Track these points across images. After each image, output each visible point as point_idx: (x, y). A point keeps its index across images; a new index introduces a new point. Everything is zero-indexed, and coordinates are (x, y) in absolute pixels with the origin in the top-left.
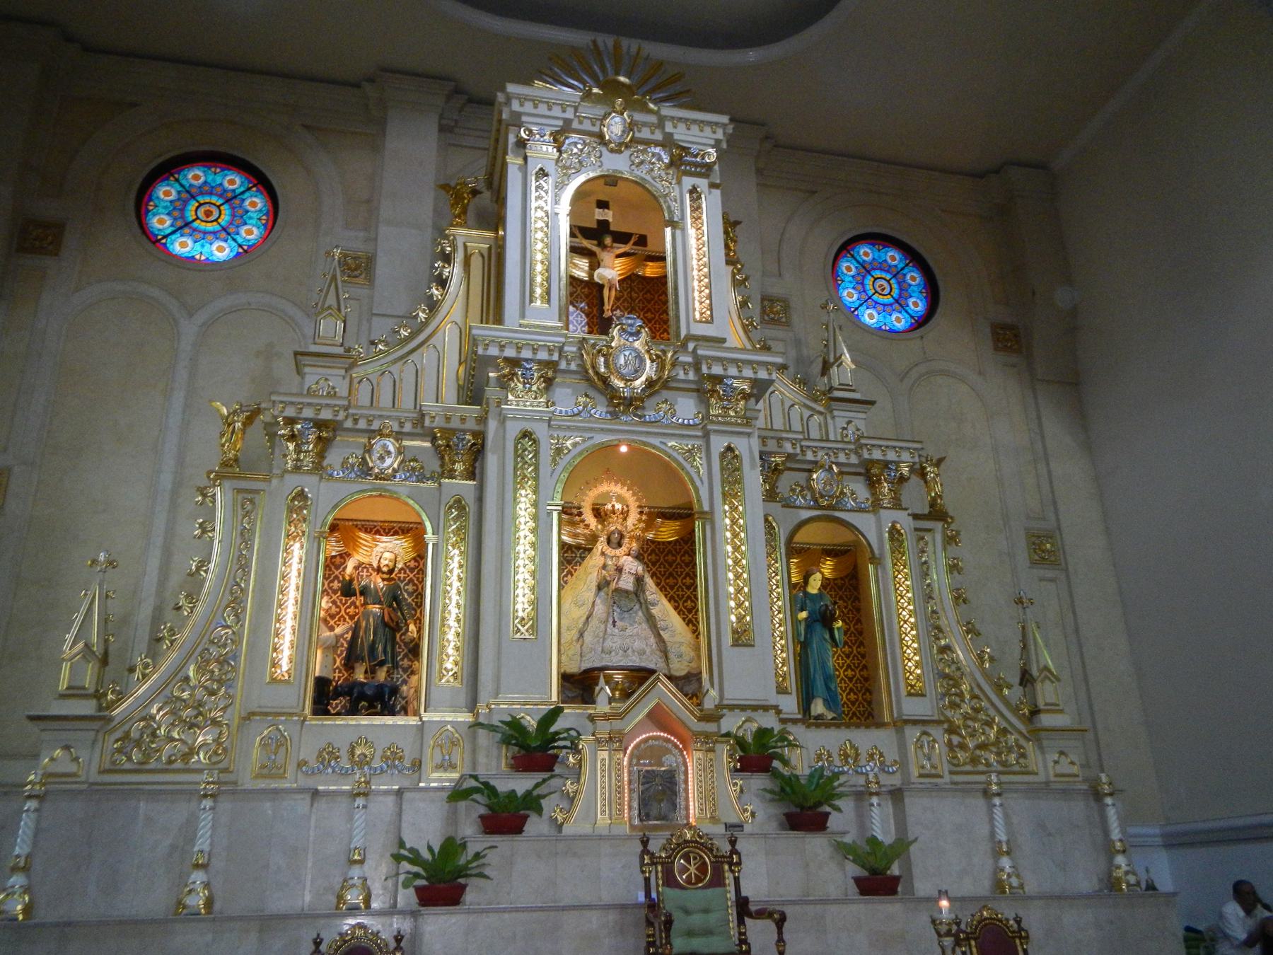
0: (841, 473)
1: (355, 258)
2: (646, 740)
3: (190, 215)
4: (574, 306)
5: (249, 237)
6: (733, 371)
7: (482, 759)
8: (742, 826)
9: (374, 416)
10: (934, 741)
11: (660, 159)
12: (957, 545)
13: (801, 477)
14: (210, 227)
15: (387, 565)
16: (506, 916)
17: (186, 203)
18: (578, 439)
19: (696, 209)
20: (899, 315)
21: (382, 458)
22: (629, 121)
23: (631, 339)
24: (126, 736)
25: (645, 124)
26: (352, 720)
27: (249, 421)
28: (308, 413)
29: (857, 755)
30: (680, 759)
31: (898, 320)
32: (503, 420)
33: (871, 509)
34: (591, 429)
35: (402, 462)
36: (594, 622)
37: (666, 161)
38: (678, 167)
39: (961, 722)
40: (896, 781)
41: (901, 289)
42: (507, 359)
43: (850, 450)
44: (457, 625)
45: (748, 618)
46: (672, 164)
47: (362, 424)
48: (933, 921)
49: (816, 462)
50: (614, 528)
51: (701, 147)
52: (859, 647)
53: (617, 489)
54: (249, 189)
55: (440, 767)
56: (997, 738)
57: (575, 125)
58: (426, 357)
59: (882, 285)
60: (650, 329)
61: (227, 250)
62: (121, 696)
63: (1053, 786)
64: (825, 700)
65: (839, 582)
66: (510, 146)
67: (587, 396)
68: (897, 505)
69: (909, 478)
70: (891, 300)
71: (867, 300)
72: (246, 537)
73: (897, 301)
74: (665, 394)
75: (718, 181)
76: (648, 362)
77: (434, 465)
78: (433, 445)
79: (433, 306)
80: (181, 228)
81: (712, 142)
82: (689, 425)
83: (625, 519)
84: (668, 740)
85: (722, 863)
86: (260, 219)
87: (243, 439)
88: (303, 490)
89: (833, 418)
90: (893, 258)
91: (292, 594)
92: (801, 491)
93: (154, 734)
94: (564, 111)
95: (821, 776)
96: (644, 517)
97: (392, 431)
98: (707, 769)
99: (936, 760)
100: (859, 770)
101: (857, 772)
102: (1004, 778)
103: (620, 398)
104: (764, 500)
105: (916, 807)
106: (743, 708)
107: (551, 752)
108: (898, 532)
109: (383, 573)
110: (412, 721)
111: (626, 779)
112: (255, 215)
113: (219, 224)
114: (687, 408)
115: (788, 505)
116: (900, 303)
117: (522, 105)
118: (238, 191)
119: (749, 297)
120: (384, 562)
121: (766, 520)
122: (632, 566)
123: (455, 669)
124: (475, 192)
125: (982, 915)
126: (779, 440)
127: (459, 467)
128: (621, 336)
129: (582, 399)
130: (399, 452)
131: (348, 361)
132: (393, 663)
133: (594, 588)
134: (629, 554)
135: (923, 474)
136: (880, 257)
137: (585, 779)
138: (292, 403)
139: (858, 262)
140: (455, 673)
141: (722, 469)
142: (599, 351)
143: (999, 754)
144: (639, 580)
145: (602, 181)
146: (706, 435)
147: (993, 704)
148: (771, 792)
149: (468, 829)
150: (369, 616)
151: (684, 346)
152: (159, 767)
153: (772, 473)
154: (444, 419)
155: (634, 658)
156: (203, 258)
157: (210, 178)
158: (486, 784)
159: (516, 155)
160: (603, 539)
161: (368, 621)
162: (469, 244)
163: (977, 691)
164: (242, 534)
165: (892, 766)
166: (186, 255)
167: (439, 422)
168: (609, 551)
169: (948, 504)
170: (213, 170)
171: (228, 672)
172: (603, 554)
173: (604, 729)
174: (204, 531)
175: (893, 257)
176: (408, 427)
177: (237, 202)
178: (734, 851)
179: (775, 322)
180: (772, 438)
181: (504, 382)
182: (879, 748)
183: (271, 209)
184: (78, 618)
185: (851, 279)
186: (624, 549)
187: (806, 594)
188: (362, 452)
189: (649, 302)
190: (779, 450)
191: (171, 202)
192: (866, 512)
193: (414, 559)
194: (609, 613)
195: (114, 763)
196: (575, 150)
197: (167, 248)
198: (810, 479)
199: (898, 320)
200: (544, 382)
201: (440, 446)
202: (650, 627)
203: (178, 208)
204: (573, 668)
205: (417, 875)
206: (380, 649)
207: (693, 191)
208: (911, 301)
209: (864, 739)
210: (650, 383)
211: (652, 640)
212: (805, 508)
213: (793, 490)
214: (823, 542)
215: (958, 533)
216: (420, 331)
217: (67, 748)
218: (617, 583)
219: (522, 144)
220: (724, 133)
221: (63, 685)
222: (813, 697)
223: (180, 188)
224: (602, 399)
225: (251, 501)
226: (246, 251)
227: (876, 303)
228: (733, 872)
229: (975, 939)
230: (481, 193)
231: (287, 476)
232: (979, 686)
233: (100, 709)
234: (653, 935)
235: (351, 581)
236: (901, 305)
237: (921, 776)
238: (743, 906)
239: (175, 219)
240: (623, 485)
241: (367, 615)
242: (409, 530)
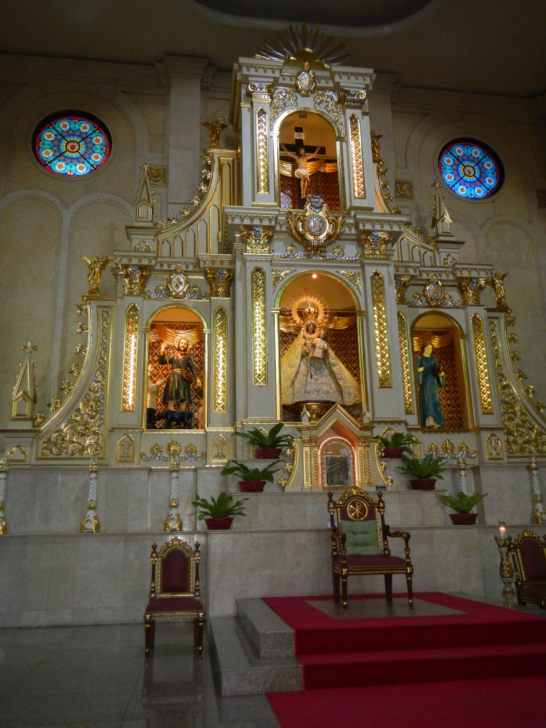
0: (443, 286)
1: (157, 170)
2: (330, 441)
3: (63, 149)
4: (284, 193)
6: (378, 227)
7: (239, 452)
8: (386, 488)
9: (171, 262)
10: (498, 439)
11: (332, 99)
12: (514, 326)
13: (420, 289)
14: (75, 155)
15: (183, 347)
16: (255, 535)
17: (60, 141)
18: (288, 271)
19: (354, 129)
20: (479, 188)
21: (177, 286)
22: (312, 76)
23: (317, 211)
24: (49, 441)
25: (322, 78)
26: (168, 432)
27: (103, 267)
28: (135, 261)
29: (453, 447)
30: (350, 451)
31: (479, 191)
32: (244, 262)
33: (462, 306)
34: (295, 265)
35: (189, 288)
36: (300, 376)
37: (336, 100)
38: (343, 104)
39: (515, 428)
40: (476, 462)
42: (245, 226)
43: (449, 272)
44: (223, 379)
45: (388, 372)
46: (339, 101)
47: (165, 267)
48: (496, 539)
49: (428, 280)
50: (310, 322)
51: (357, 90)
52: (454, 387)
53: (311, 300)
54: (95, 131)
55: (217, 456)
56: (536, 437)
57: (281, 81)
58: (200, 226)
59: (469, 170)
60: (329, 204)
61: (85, 169)
62: (44, 420)
64: (434, 417)
65: (443, 350)
66: (242, 97)
67: (292, 245)
68: (477, 303)
69: (485, 287)
70: (475, 179)
71: (460, 180)
72: (105, 332)
74: (338, 243)
75: (368, 111)
76: (327, 224)
77: (206, 289)
78: (205, 276)
79: (202, 196)
80: (58, 157)
81: (363, 86)
82: (352, 260)
83: (316, 317)
84: (343, 441)
85: (374, 507)
86: (102, 149)
88: (134, 306)
89: (439, 253)
91: (132, 363)
92: (420, 297)
93: (63, 440)
94: (273, 73)
95: (431, 459)
96: (327, 316)
97: (182, 270)
98: (365, 457)
99: (499, 450)
100: (454, 456)
101: (453, 457)
102: (539, 460)
103: (311, 246)
104: (397, 304)
105: (486, 476)
106: (386, 423)
107: (277, 448)
108: (478, 319)
109: (181, 351)
110: (201, 432)
111: (320, 462)
112: (98, 147)
113: (79, 153)
115: (412, 305)
116: (480, 181)
117: (248, 70)
118: (88, 133)
119: (387, 182)
120: (181, 345)
121: (399, 315)
122: (321, 343)
123: (223, 403)
124: (223, 126)
125: (524, 535)
126: (406, 267)
127: (220, 290)
128: (311, 209)
129: (289, 248)
130: (187, 282)
131: (156, 230)
132: (189, 400)
133: (299, 357)
134: (319, 337)
135: (493, 284)
136: (467, 152)
137: (297, 463)
138: (125, 256)
140: (223, 405)
141: (372, 285)
142: (299, 219)
143: (536, 446)
144: (325, 352)
145: (298, 115)
146: (363, 266)
147: (534, 418)
148: (402, 468)
149: (233, 489)
150: (175, 375)
151: (349, 213)
152: (68, 456)
153: (402, 287)
154: (211, 263)
155: (323, 396)
156: (72, 174)
158: (242, 465)
159: (246, 102)
160: (304, 329)
161: (174, 378)
162: (221, 158)
163: (525, 411)
164: (103, 330)
165: (473, 454)
166: (62, 172)
167: (208, 264)
168: (308, 336)
169: (509, 302)
170: (74, 121)
171: (100, 406)
172: (304, 337)
173: (306, 435)
174: (83, 330)
175: (476, 152)
176: (191, 268)
178: (381, 501)
179: (403, 196)
180: (402, 266)
181: (244, 240)
182: (466, 444)
183: (108, 142)
184: (19, 377)
185: (450, 167)
186: (316, 334)
187: (423, 357)
188: (166, 283)
189: (328, 188)
190: (407, 273)
191: (52, 141)
192: (458, 308)
193: (198, 343)
194: (308, 371)
195: (43, 454)
196: (281, 97)
197: (52, 169)
198: (424, 290)
199: (479, 191)
200: (267, 239)
201: (209, 278)
202: (332, 378)
203: (55, 145)
204: (289, 402)
205: (206, 513)
206: (182, 392)
207: (353, 117)
208: (487, 179)
209: (457, 439)
210: (329, 237)
211: (333, 386)
212: (423, 307)
213: (415, 297)
214: (434, 326)
215: (514, 319)
216: (195, 211)
217: (19, 446)
218: (313, 354)
219: (249, 95)
220: (371, 81)
221: (14, 414)
222: (427, 416)
224: (300, 247)
225: (107, 312)
226: (95, 169)
227: (466, 181)
228: (380, 512)
229: (519, 548)
230: (227, 126)
231: (125, 298)
232: (526, 408)
233: (34, 426)
234: (336, 546)
235: (164, 355)
236: (481, 182)
238: (386, 530)
239: (55, 151)
240: (315, 297)
241: (173, 374)
242: (194, 327)
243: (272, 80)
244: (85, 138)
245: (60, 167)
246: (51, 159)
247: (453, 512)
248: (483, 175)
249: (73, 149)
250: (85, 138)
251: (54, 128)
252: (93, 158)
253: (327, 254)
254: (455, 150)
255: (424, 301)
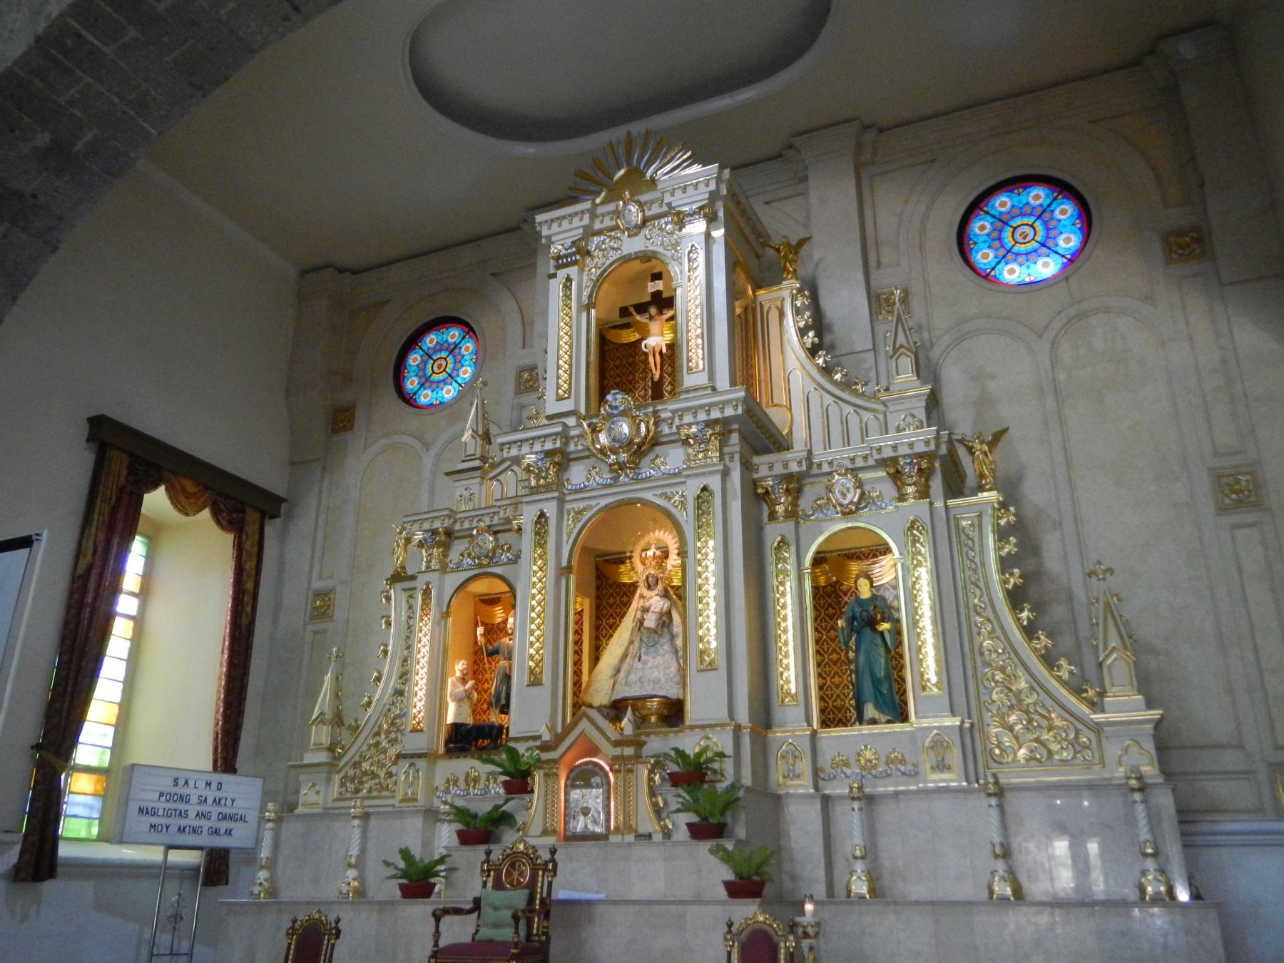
3: (429, 372)
5: (465, 376)
14: (441, 377)
17: (424, 363)
28: (426, 526)
36: (628, 659)
41: (1048, 229)
47: (466, 525)
54: (464, 337)
74: (658, 449)
81: (707, 196)
85: (539, 869)
87: (406, 551)
134: (657, 595)
139: (993, 217)
168: (647, 593)
175: (1037, 195)
176: (496, 520)
177: (457, 351)
178: (553, 860)
186: (656, 592)
199: (1046, 265)
211: (674, 669)
222: (864, 702)
227: (1017, 254)
233: (335, 758)
239: (420, 378)
243: (581, 231)
246: (416, 389)
247: (730, 876)
248: (1052, 233)
249: (439, 368)
250: (453, 349)
251: (420, 348)
253: (642, 471)
254: (993, 205)
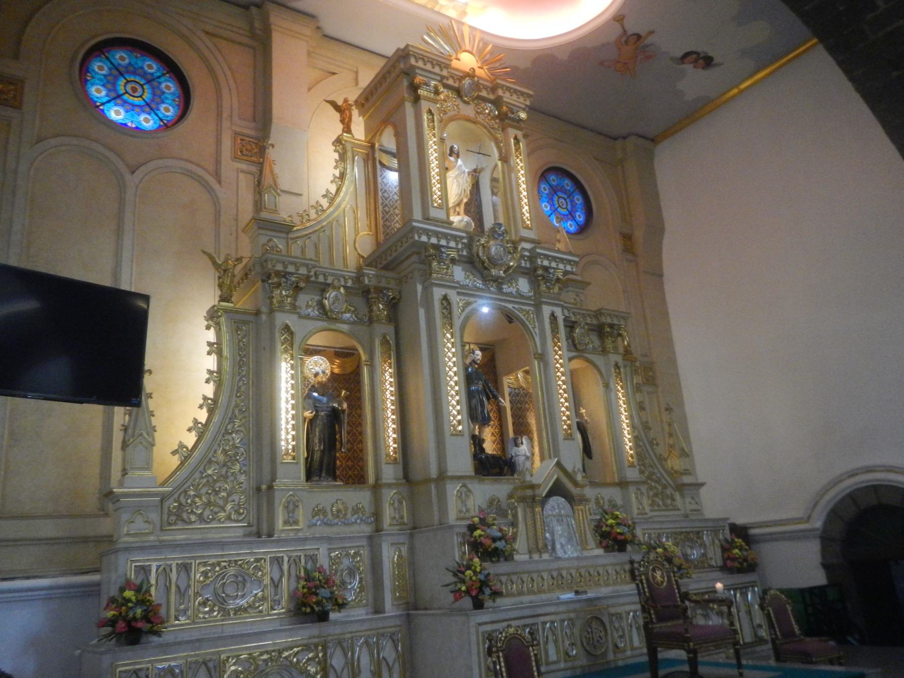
3: (121, 90)
6: (554, 265)
14: (137, 101)
17: (116, 79)
31: (571, 225)
54: (164, 75)
61: (151, 122)
63: (691, 517)
68: (616, 350)
73: (570, 213)
80: (114, 99)
90: (567, 185)
113: (144, 100)
114: (524, 285)
116: (571, 215)
117: (417, 61)
143: (663, 500)
146: (538, 306)
157: (133, 61)
175: (567, 184)
177: (155, 84)
191: (105, 76)
203: (110, 83)
208: (577, 214)
223: (111, 66)
237: (638, 514)
239: (109, 90)
244: (150, 80)
245: (117, 113)
252: (162, 109)
255: (571, 343)
